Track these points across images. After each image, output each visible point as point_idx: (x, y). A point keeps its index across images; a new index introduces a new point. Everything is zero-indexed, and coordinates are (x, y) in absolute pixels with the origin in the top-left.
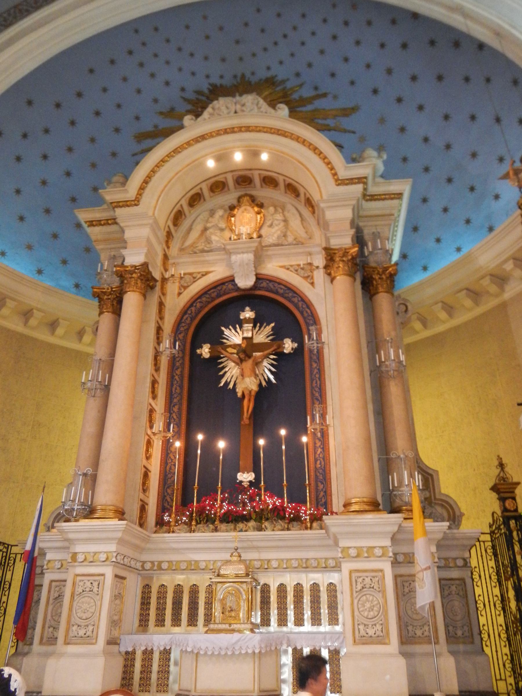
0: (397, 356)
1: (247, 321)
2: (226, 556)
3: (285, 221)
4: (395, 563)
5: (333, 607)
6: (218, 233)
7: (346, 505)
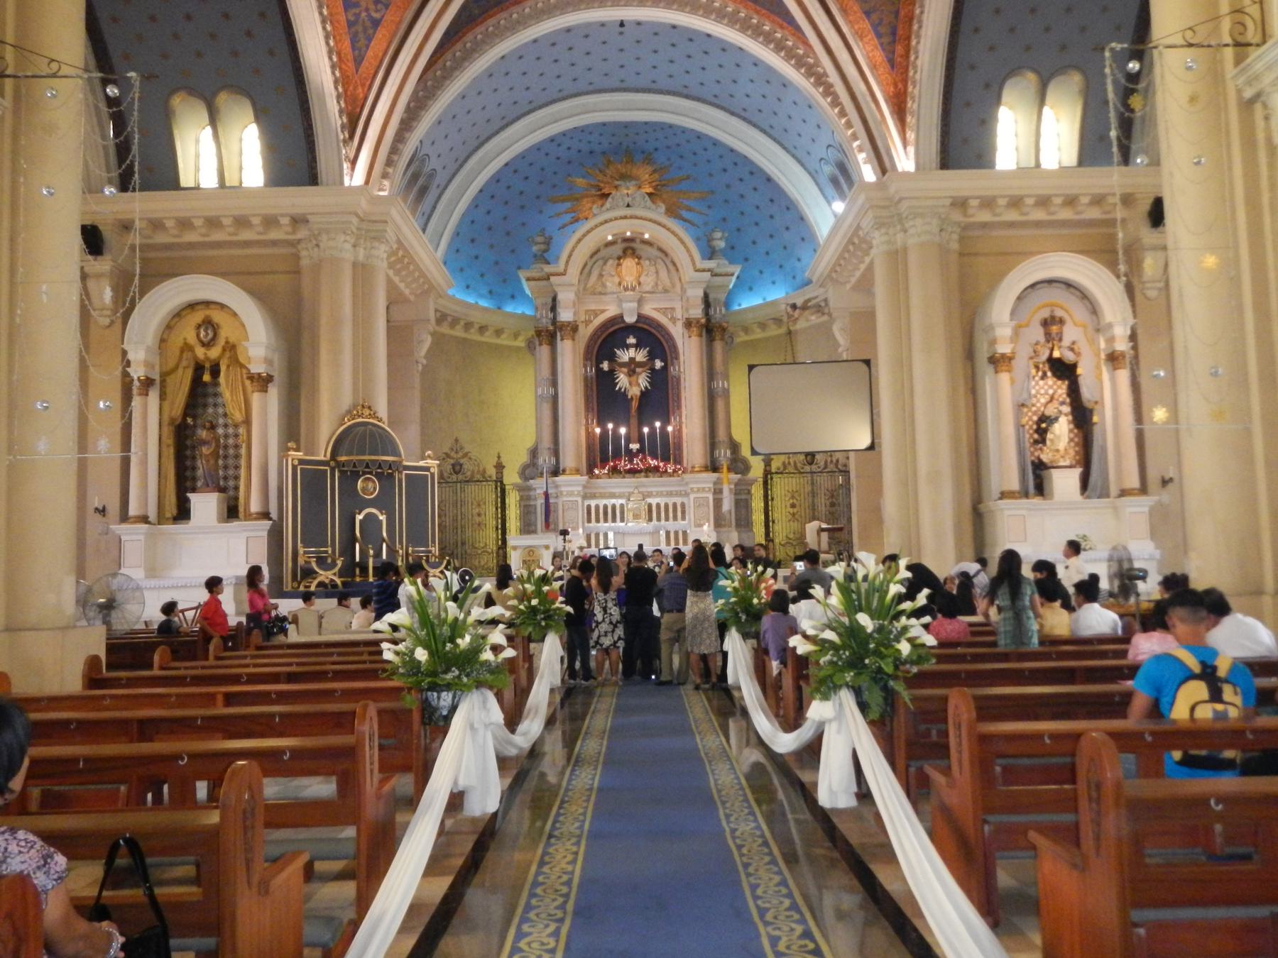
0: (723, 384)
2: (631, 490)
3: (657, 272)
4: (715, 493)
5: (683, 512)
6: (610, 279)
7: (693, 467)
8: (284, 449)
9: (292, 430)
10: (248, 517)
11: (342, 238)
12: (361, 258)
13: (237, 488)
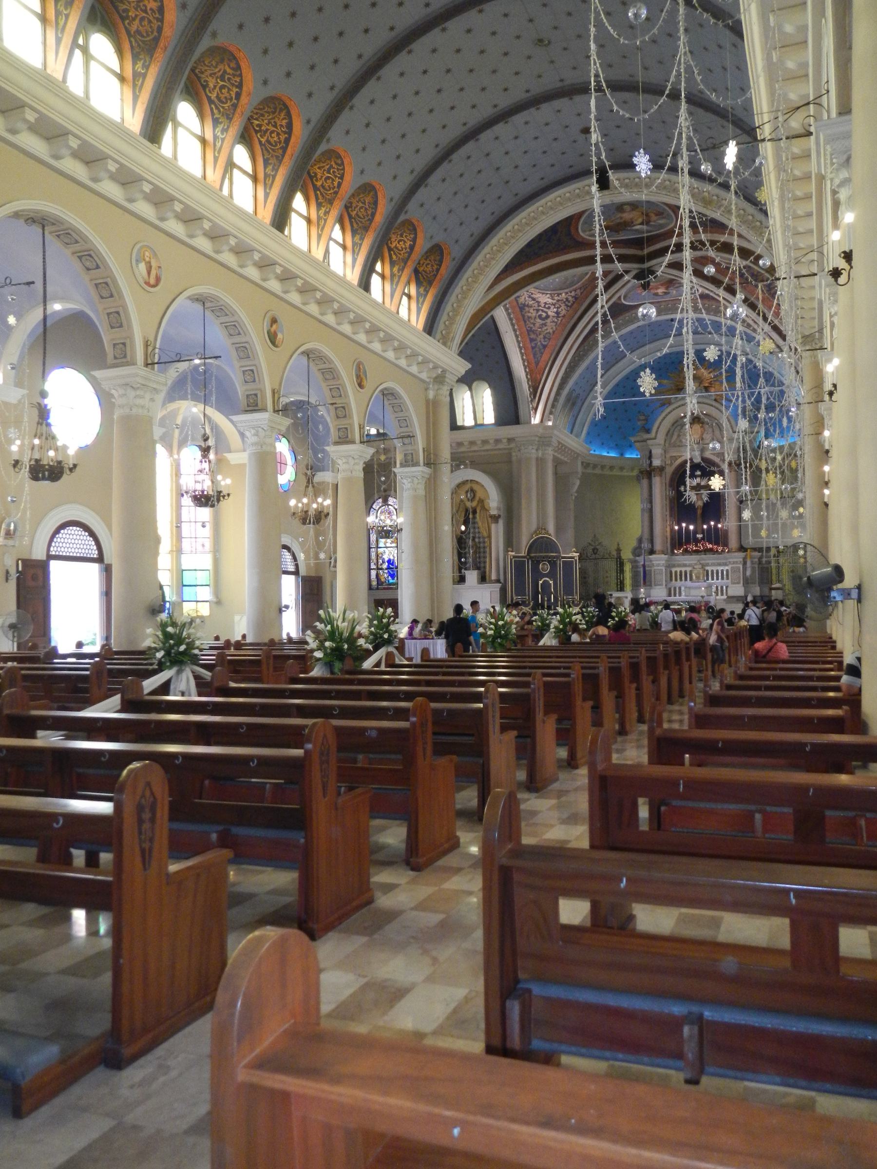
1: (698, 476)
8: (506, 551)
9: (509, 543)
10: (491, 582)
11: (531, 447)
12: (540, 455)
13: (485, 567)
